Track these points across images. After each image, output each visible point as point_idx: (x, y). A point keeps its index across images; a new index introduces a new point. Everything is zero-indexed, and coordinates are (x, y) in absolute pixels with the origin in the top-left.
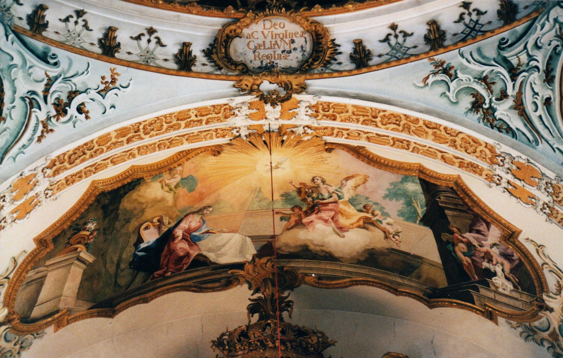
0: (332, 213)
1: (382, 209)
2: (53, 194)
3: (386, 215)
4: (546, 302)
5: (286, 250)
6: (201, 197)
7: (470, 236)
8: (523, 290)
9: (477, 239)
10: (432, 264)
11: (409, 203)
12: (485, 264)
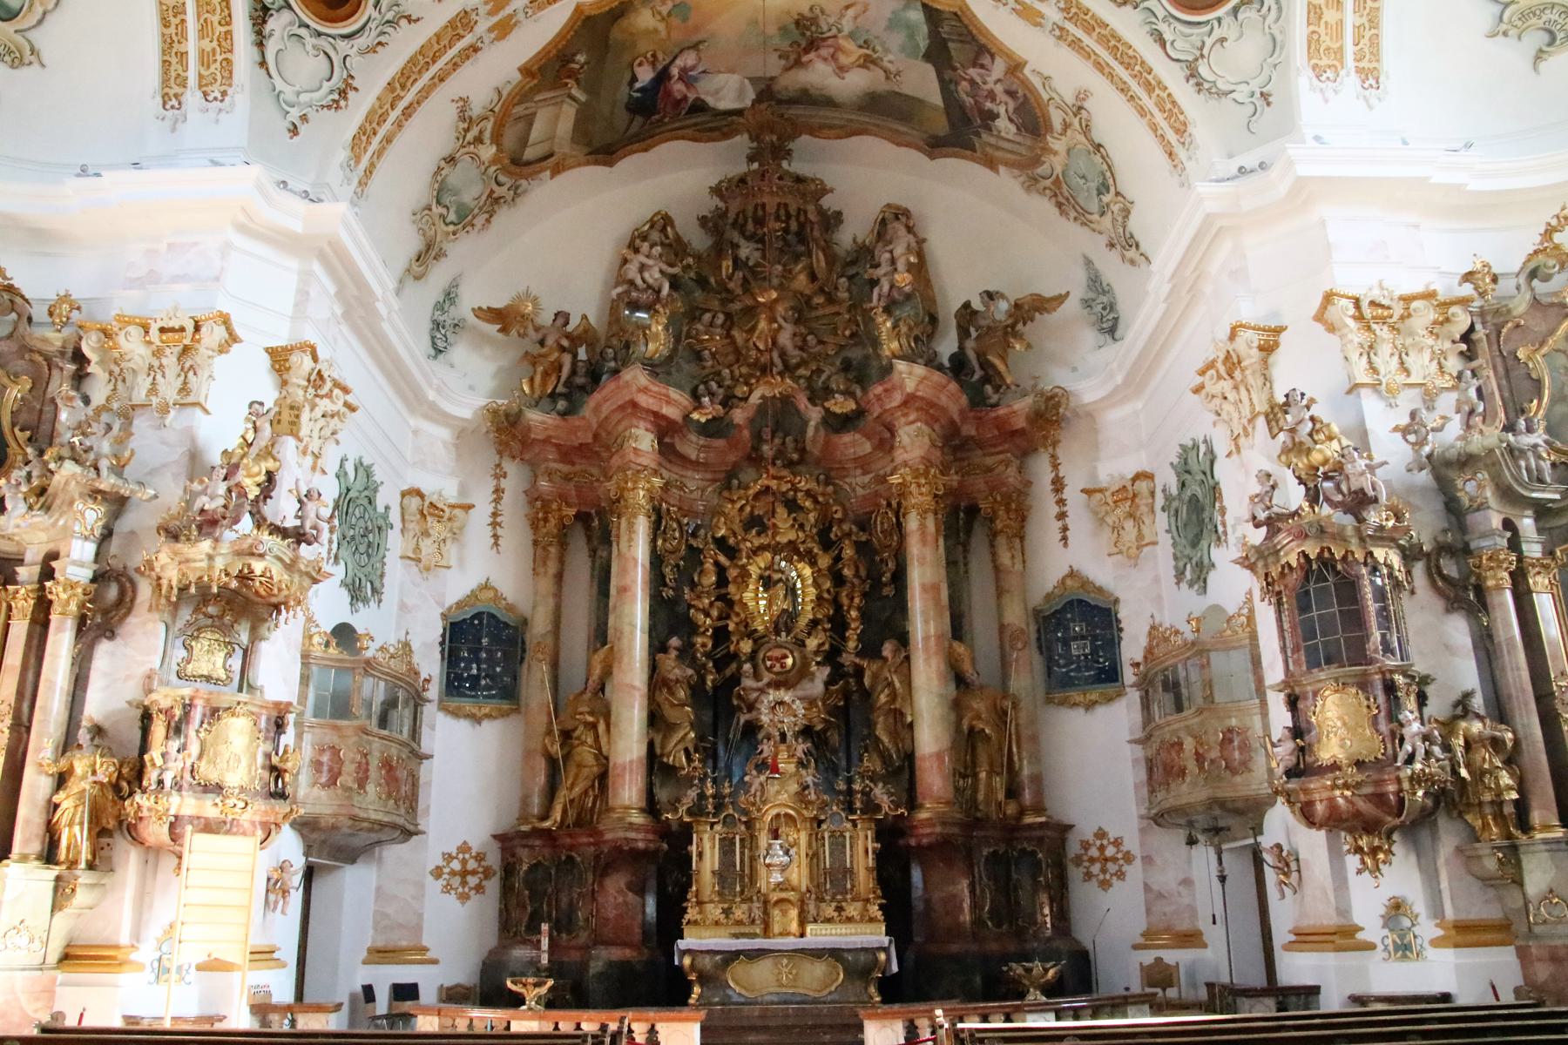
0: (832, 50)
1: (883, 44)
2: (534, 13)
3: (887, 51)
5: (784, 96)
6: (697, 29)
11: (911, 36)
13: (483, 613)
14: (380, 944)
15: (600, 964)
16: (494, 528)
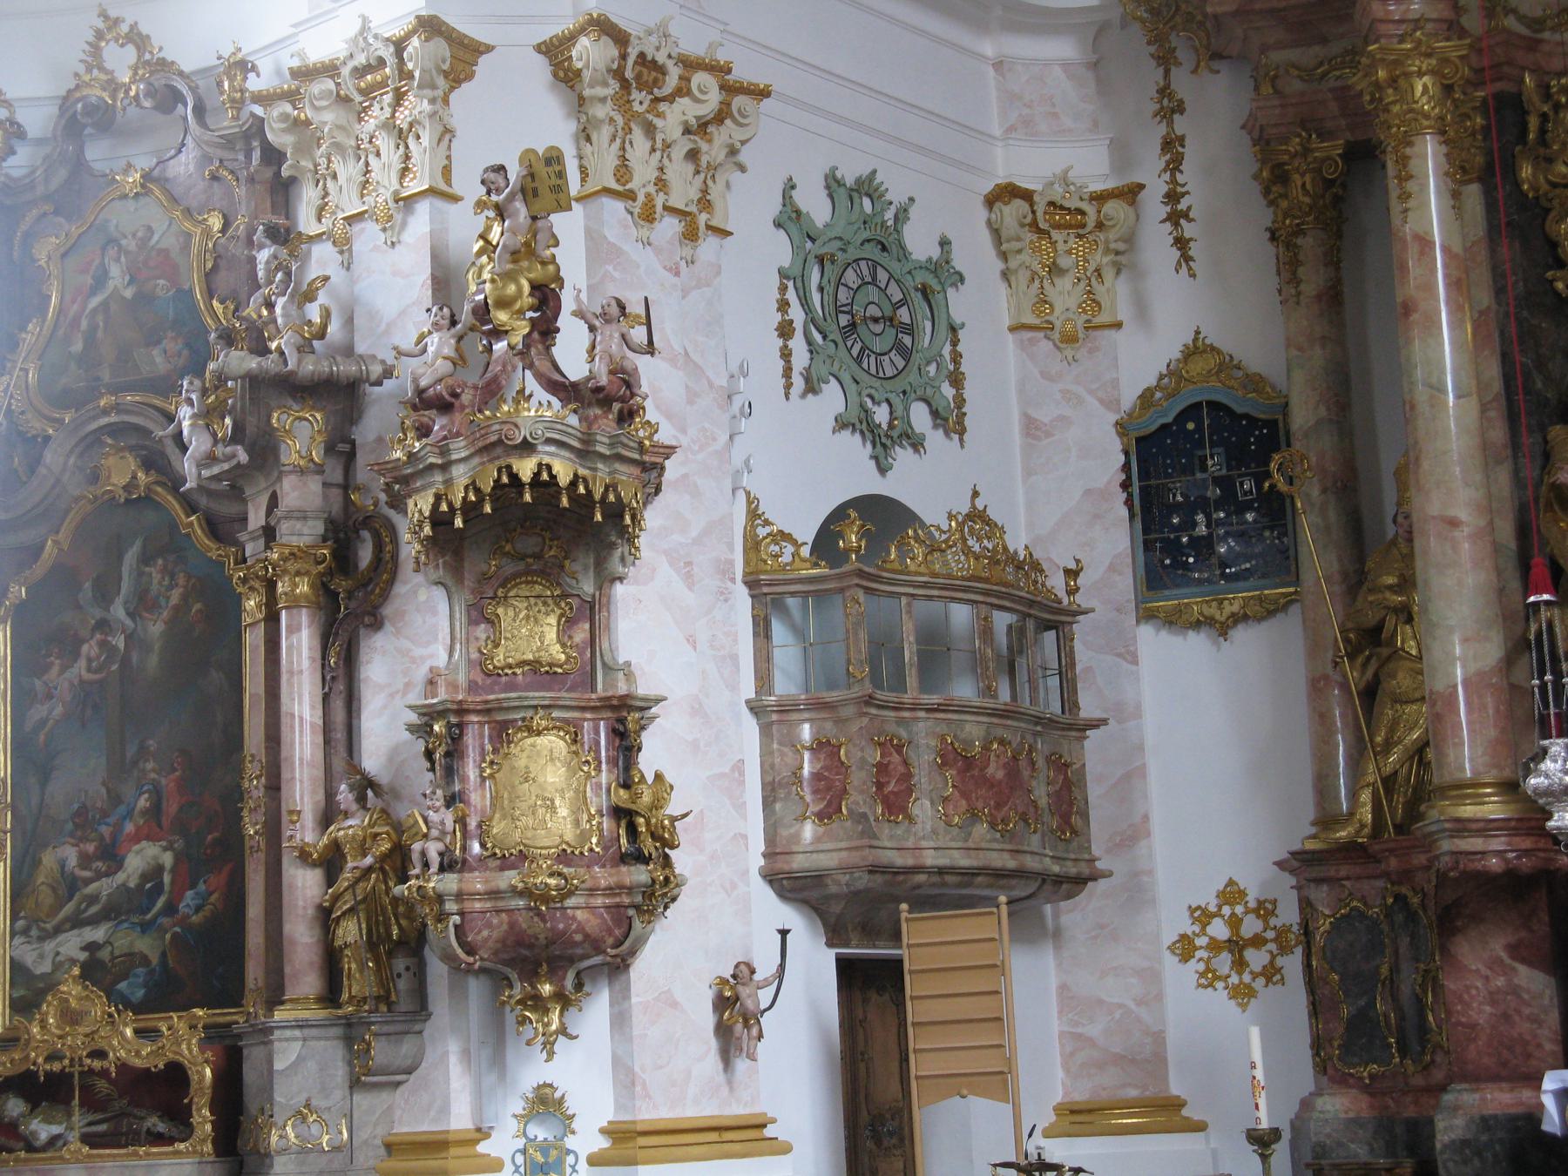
13: (1198, 406)
14: (1081, 1095)
15: (1459, 1122)
16: (1177, 225)
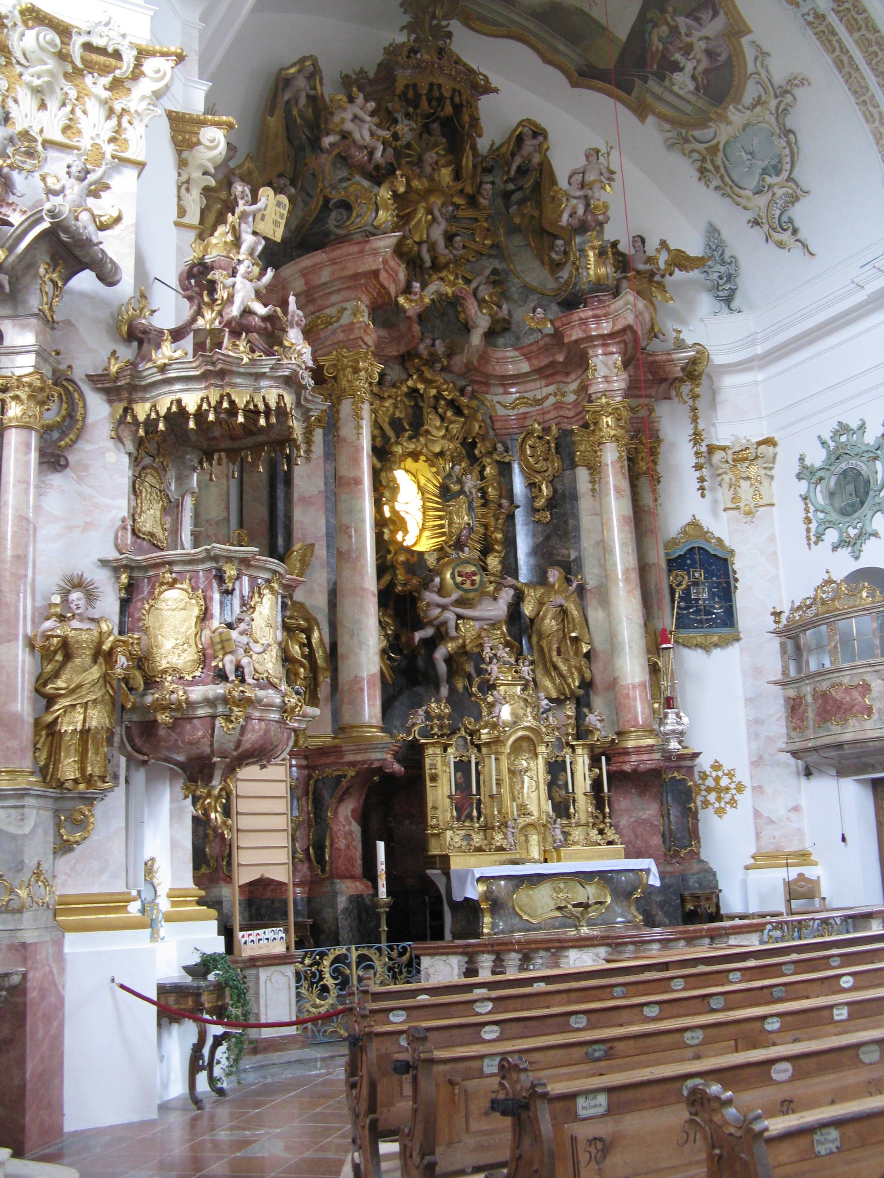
4: (729, 114)
7: (682, 22)
8: (704, 94)
9: (689, 27)
10: (612, 40)
12: (678, 57)
